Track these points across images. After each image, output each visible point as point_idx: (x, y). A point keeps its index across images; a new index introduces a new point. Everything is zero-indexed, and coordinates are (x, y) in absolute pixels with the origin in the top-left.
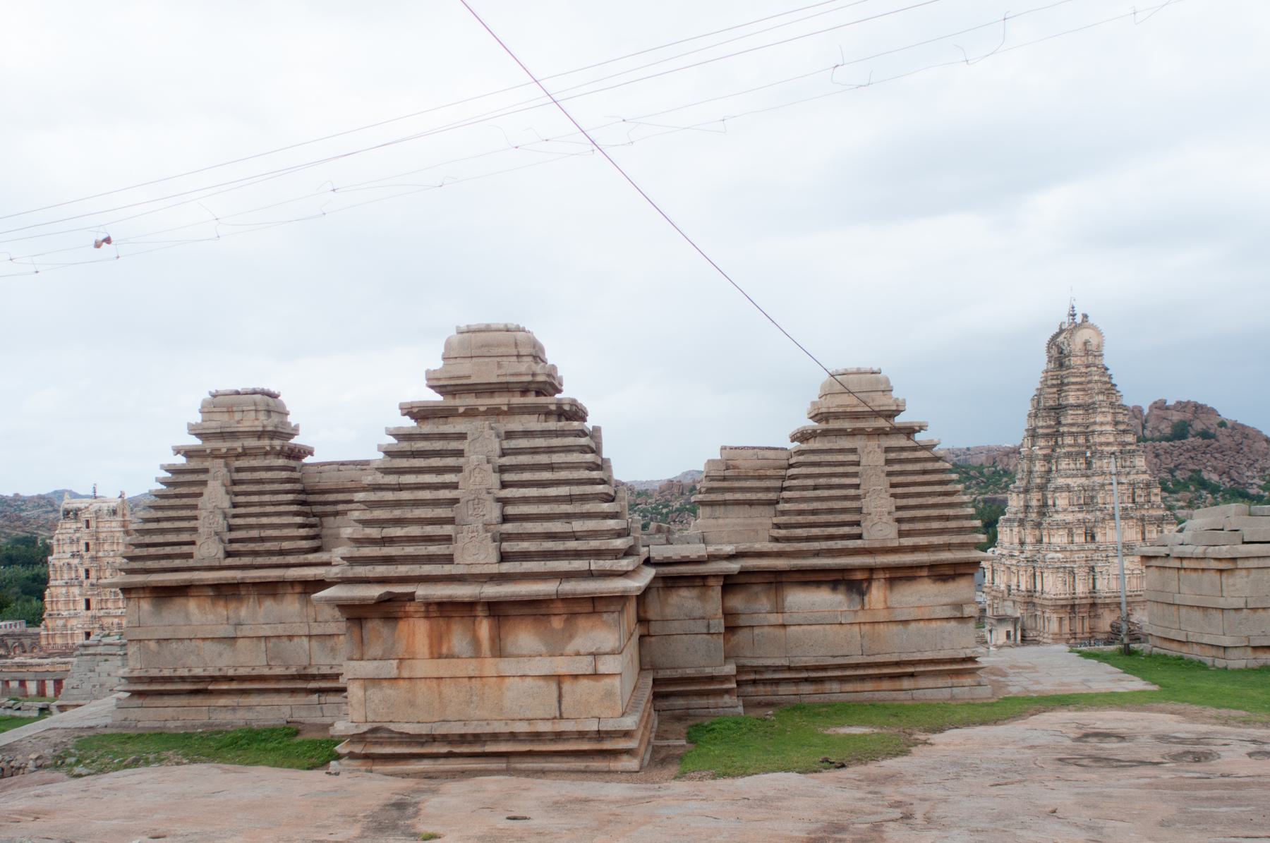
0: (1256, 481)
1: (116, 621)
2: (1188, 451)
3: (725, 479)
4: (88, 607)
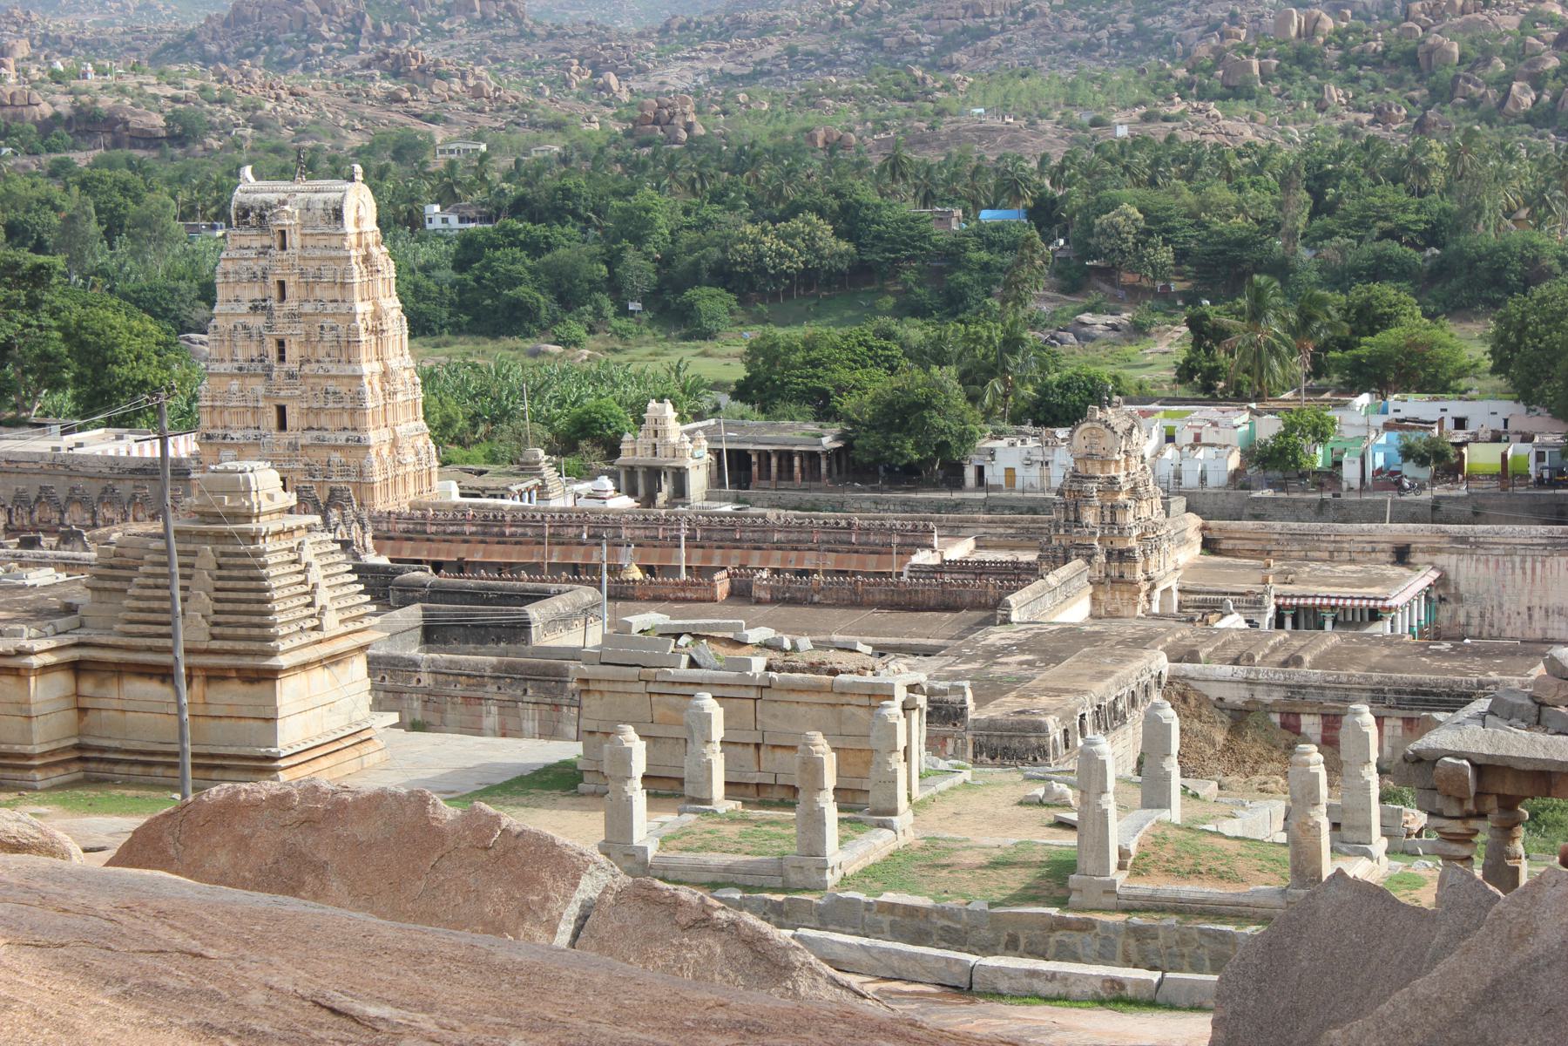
1: (336, 457)
3: (112, 567)
4: (282, 425)
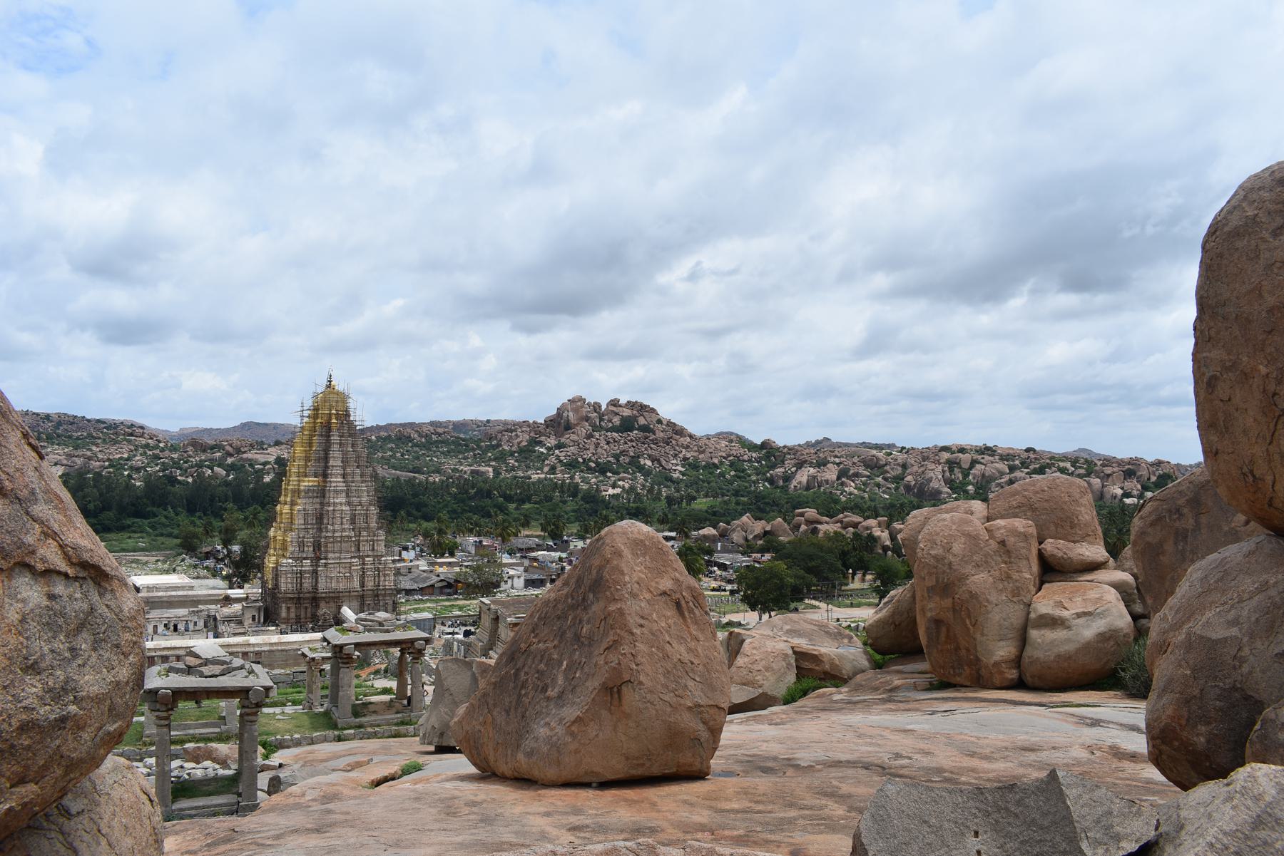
0: (679, 468)
2: (631, 441)
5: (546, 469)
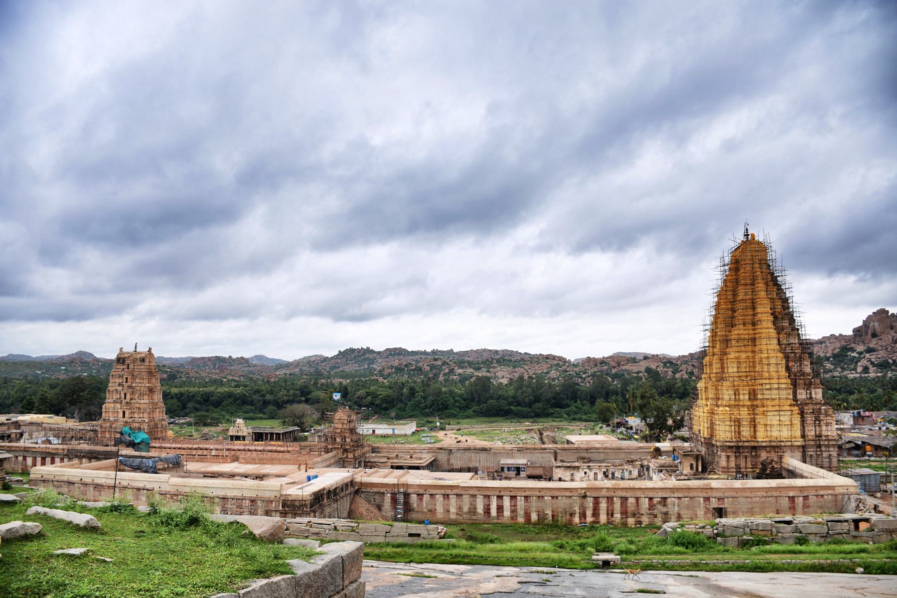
4: (124, 417)
5: (859, 369)
